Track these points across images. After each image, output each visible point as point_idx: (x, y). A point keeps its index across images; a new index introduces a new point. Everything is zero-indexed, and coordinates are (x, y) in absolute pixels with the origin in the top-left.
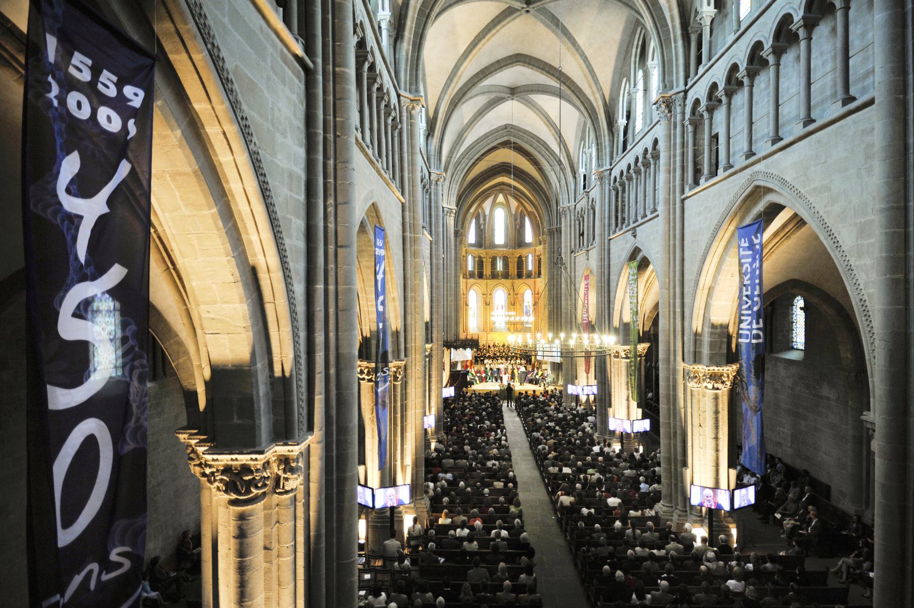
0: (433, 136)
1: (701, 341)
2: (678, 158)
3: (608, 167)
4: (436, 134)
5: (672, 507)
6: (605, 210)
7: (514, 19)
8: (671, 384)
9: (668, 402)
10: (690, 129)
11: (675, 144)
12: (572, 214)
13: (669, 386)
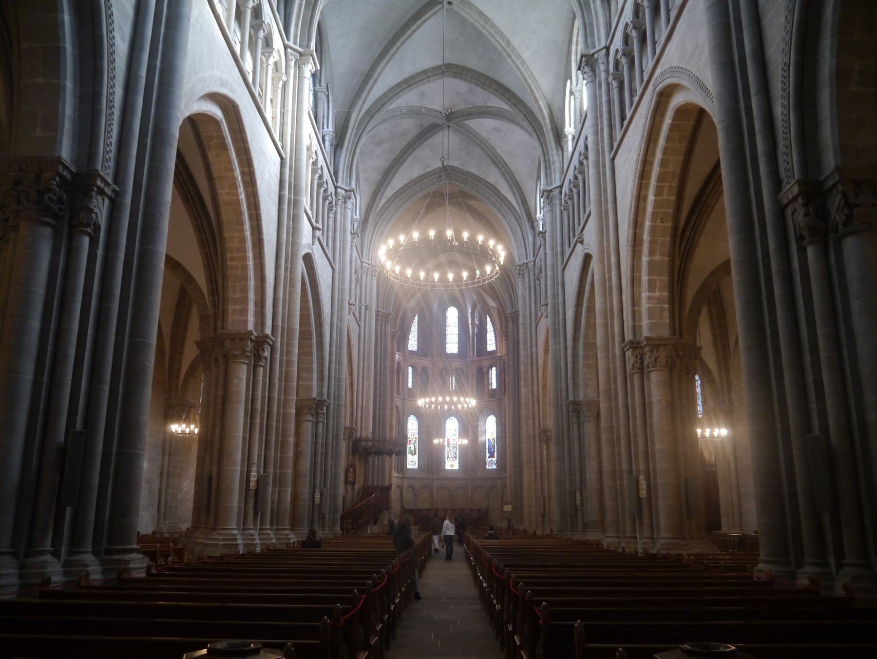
0: (342, 146)
1: (640, 312)
2: (605, 116)
3: (558, 184)
4: (346, 144)
5: (619, 537)
6: (556, 236)
7: (435, 13)
8: (612, 375)
9: (609, 399)
10: (615, 84)
11: (601, 104)
12: (532, 273)
13: (610, 378)
